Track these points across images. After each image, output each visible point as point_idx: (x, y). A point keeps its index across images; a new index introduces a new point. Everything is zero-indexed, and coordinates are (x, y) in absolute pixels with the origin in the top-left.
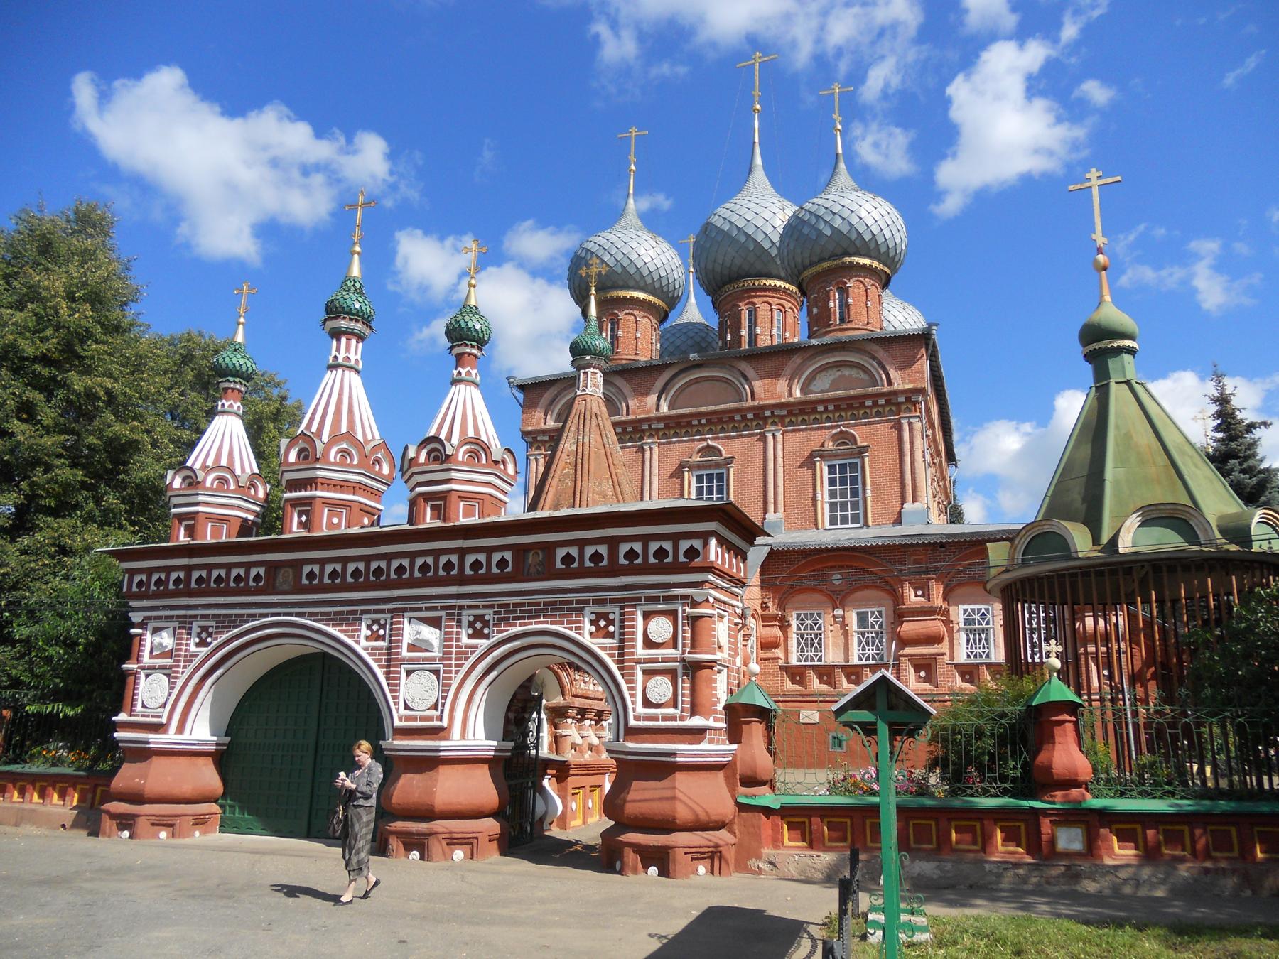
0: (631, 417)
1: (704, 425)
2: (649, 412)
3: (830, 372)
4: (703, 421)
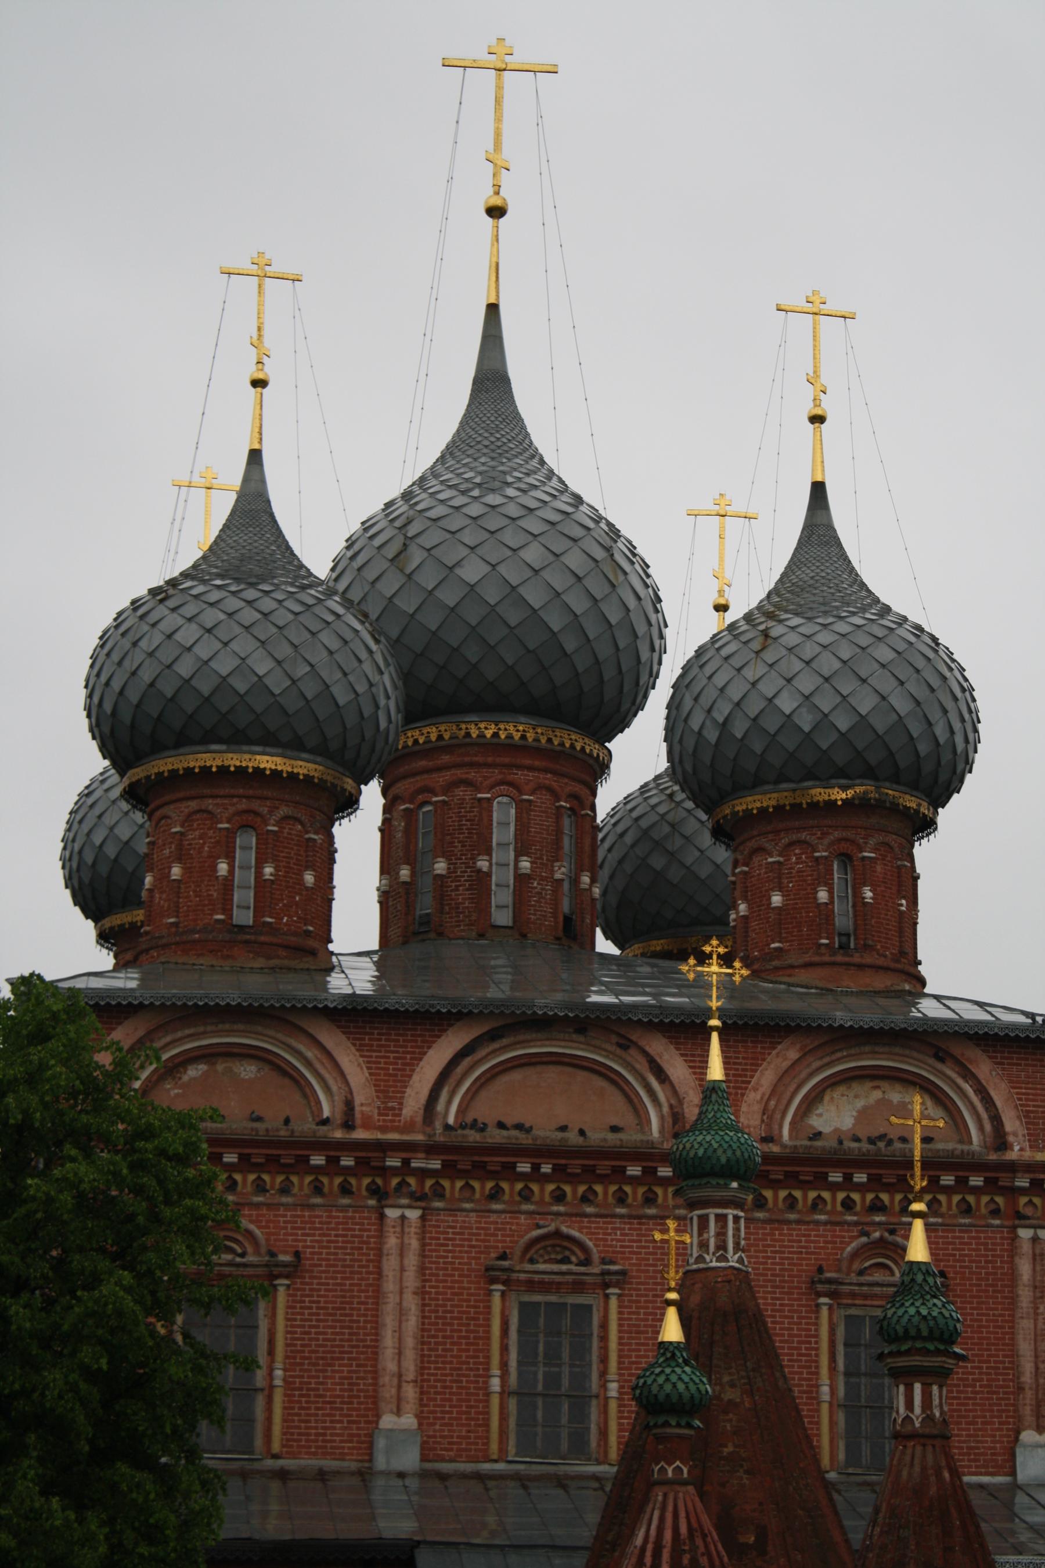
0: (360, 1134)
1: (546, 1178)
2: (409, 1127)
3: (856, 1087)
4: (546, 1169)
